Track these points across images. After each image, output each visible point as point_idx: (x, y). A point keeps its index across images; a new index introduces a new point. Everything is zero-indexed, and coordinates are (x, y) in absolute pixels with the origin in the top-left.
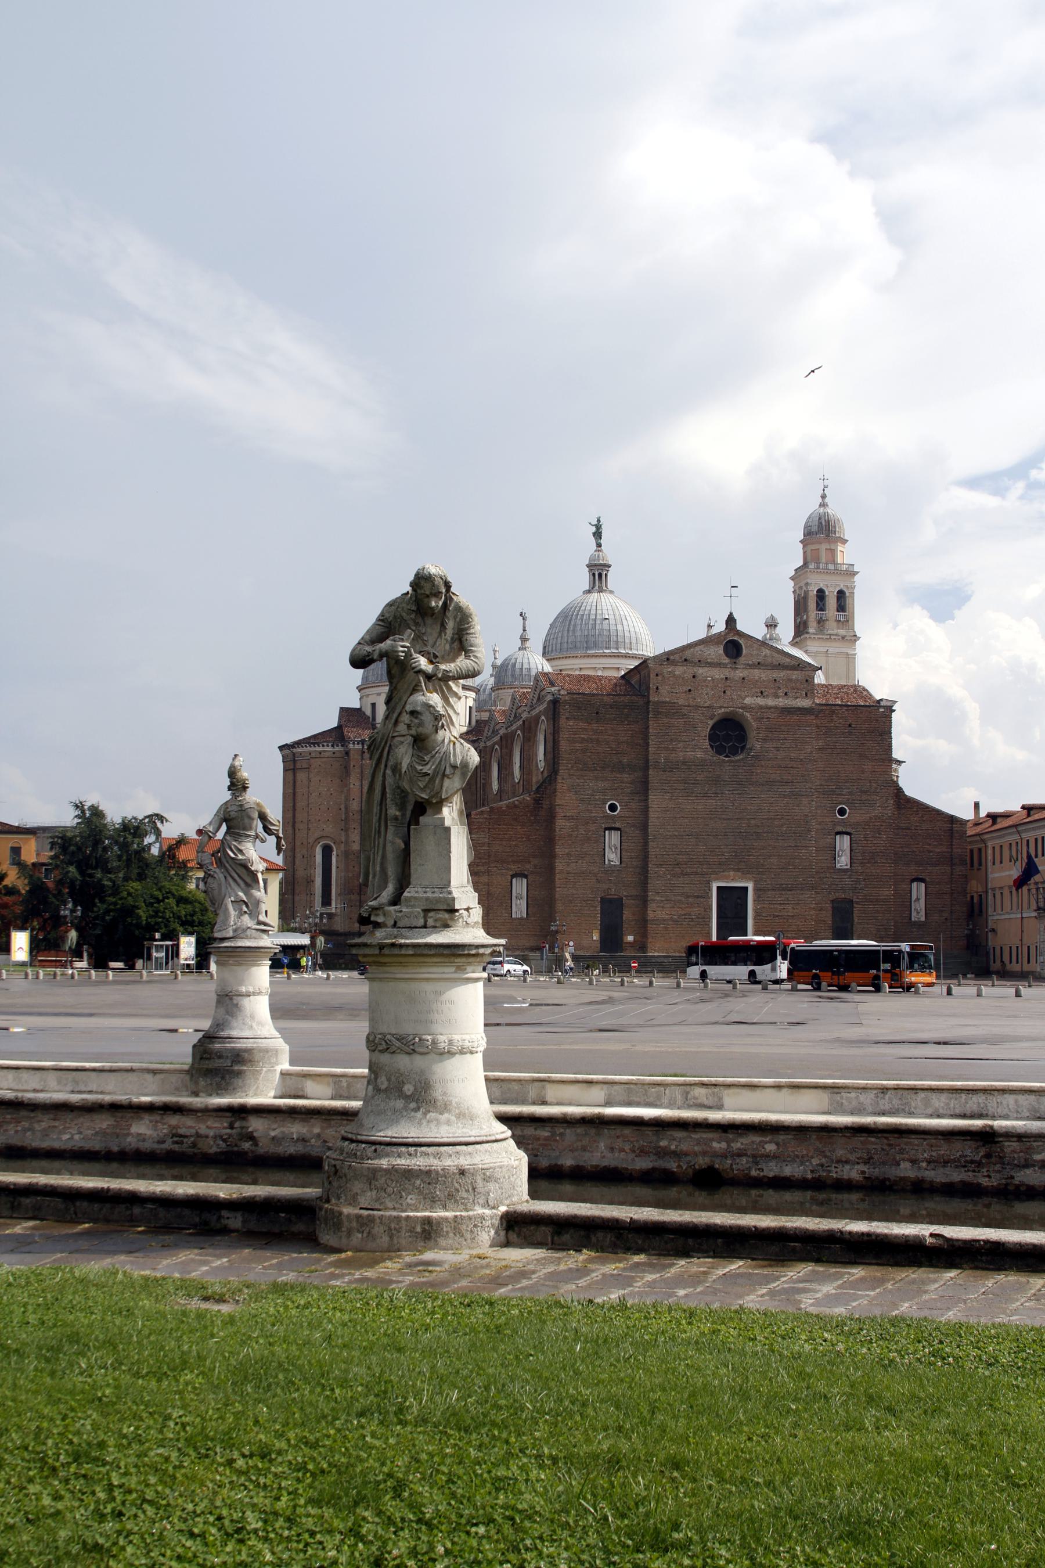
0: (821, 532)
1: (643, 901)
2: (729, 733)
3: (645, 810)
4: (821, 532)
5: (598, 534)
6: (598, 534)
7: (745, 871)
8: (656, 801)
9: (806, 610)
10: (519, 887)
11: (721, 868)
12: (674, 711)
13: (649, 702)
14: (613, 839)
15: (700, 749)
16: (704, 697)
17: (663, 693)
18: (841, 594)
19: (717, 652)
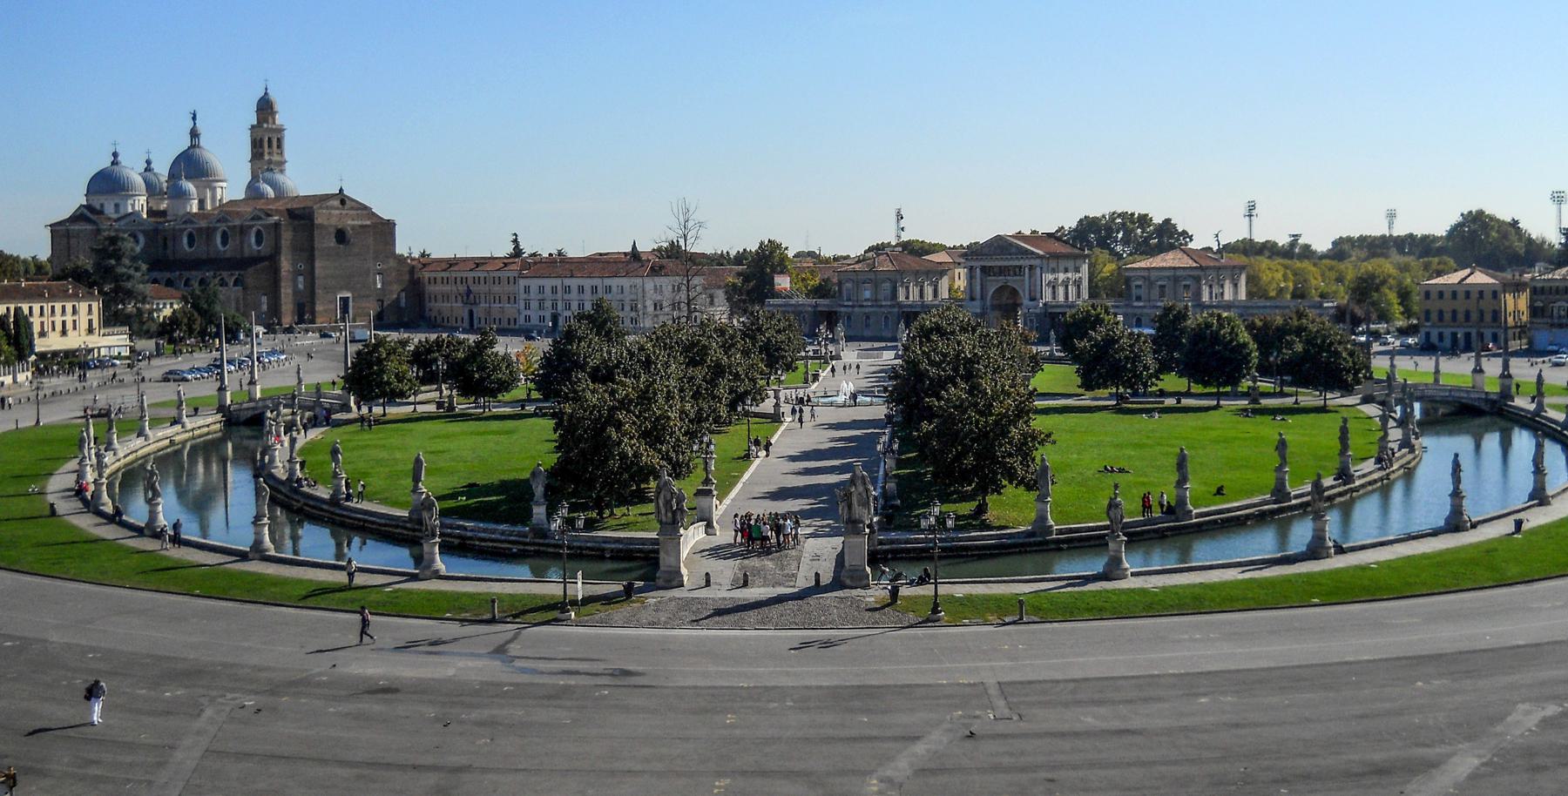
0: (265, 108)
1: (313, 303)
2: (341, 236)
3: (313, 268)
4: (265, 108)
5: (194, 118)
6: (194, 118)
7: (348, 289)
8: (318, 264)
9: (261, 146)
10: (264, 299)
11: (341, 289)
12: (321, 226)
13: (313, 225)
14: (301, 279)
15: (332, 243)
16: (333, 221)
17: (319, 220)
18: (279, 141)
19: (336, 203)
